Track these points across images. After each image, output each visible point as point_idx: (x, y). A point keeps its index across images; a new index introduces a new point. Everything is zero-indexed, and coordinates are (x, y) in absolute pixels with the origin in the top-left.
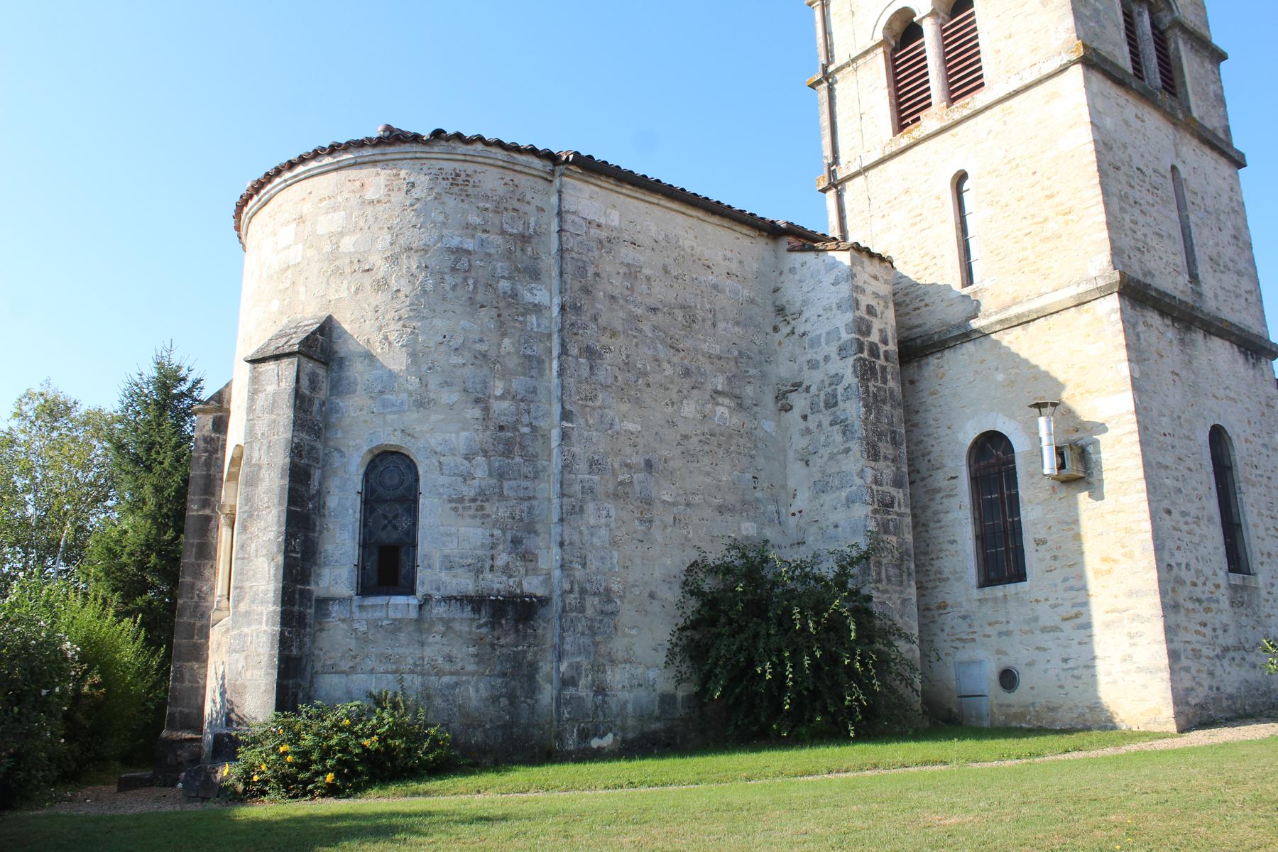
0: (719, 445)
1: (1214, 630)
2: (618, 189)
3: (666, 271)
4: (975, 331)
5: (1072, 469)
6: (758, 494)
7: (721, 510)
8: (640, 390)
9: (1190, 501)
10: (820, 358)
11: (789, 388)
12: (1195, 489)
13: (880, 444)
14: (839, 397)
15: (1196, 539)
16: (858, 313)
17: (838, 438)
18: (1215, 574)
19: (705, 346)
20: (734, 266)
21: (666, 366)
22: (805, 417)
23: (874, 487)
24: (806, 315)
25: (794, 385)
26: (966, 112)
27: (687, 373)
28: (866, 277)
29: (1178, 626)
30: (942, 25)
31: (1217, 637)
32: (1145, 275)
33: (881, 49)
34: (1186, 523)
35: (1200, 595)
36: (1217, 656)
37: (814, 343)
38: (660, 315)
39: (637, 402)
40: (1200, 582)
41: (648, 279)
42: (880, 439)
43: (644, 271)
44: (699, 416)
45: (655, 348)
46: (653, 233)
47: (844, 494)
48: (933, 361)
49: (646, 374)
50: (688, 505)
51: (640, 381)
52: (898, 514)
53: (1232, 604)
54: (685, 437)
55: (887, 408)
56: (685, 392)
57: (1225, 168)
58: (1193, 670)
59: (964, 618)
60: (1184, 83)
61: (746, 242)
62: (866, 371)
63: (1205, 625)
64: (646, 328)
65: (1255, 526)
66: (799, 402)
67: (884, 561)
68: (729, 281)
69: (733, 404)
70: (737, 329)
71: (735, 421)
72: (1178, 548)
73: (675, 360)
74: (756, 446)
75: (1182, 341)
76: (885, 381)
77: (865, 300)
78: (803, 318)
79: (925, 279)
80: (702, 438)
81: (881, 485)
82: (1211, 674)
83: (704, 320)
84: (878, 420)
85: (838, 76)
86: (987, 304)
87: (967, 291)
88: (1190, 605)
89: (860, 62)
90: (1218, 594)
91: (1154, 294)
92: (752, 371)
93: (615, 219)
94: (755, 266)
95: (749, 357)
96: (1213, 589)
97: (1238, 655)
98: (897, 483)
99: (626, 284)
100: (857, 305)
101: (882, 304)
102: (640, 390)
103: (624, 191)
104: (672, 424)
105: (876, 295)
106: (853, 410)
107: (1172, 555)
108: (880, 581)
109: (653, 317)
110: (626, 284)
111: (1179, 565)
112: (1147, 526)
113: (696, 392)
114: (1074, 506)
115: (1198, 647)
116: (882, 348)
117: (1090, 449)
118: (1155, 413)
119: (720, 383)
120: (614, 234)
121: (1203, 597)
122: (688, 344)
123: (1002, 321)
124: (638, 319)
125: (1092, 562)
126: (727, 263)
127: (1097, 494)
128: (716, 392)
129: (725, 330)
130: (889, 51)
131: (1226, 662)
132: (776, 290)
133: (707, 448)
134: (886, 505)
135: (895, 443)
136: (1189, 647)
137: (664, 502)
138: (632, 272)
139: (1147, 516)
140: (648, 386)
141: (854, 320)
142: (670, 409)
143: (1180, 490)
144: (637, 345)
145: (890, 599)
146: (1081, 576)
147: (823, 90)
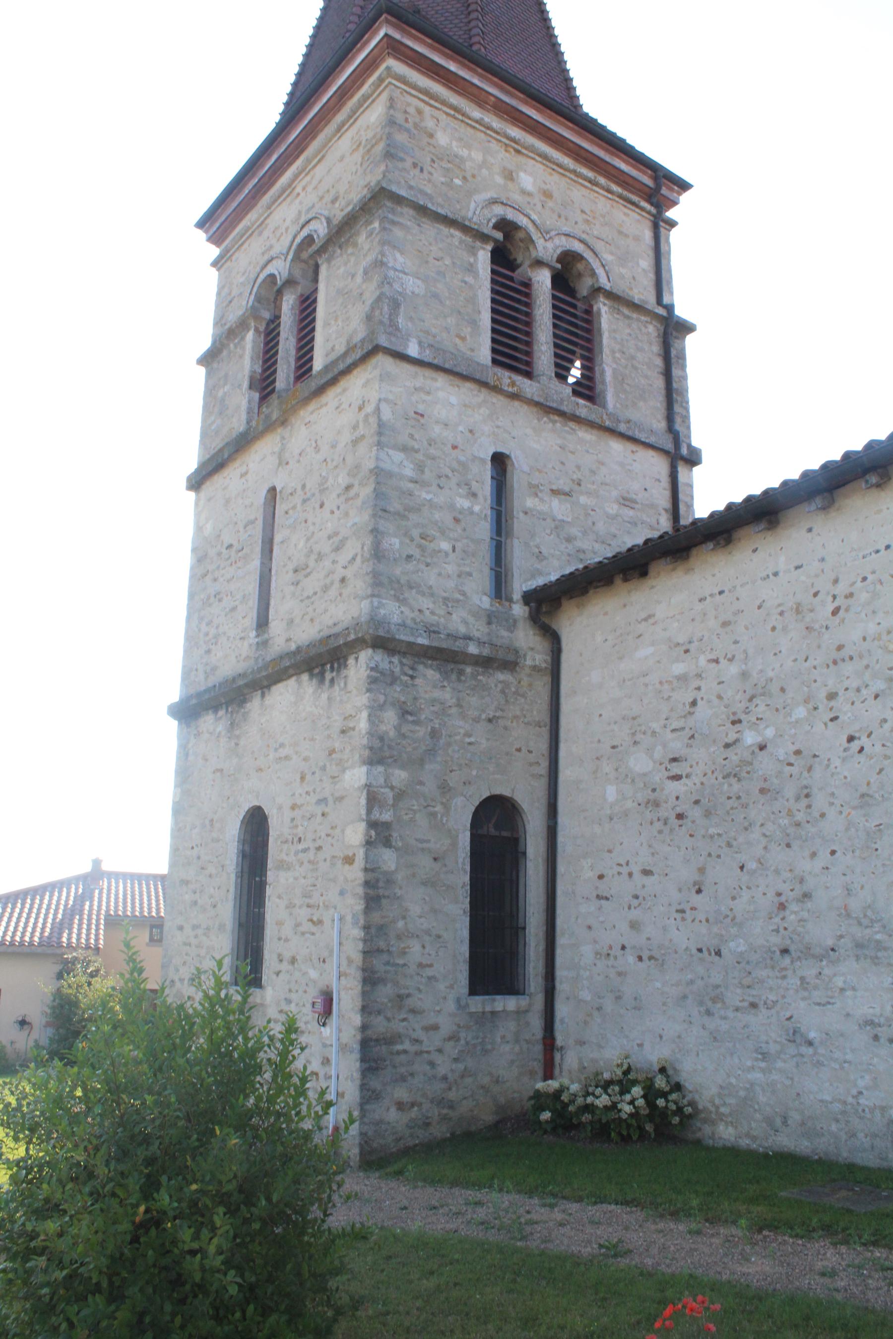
12: (211, 897)
65: (280, 923)
72: (184, 963)
75: (233, 725)
107: (177, 970)
111: (182, 980)
143: (196, 903)
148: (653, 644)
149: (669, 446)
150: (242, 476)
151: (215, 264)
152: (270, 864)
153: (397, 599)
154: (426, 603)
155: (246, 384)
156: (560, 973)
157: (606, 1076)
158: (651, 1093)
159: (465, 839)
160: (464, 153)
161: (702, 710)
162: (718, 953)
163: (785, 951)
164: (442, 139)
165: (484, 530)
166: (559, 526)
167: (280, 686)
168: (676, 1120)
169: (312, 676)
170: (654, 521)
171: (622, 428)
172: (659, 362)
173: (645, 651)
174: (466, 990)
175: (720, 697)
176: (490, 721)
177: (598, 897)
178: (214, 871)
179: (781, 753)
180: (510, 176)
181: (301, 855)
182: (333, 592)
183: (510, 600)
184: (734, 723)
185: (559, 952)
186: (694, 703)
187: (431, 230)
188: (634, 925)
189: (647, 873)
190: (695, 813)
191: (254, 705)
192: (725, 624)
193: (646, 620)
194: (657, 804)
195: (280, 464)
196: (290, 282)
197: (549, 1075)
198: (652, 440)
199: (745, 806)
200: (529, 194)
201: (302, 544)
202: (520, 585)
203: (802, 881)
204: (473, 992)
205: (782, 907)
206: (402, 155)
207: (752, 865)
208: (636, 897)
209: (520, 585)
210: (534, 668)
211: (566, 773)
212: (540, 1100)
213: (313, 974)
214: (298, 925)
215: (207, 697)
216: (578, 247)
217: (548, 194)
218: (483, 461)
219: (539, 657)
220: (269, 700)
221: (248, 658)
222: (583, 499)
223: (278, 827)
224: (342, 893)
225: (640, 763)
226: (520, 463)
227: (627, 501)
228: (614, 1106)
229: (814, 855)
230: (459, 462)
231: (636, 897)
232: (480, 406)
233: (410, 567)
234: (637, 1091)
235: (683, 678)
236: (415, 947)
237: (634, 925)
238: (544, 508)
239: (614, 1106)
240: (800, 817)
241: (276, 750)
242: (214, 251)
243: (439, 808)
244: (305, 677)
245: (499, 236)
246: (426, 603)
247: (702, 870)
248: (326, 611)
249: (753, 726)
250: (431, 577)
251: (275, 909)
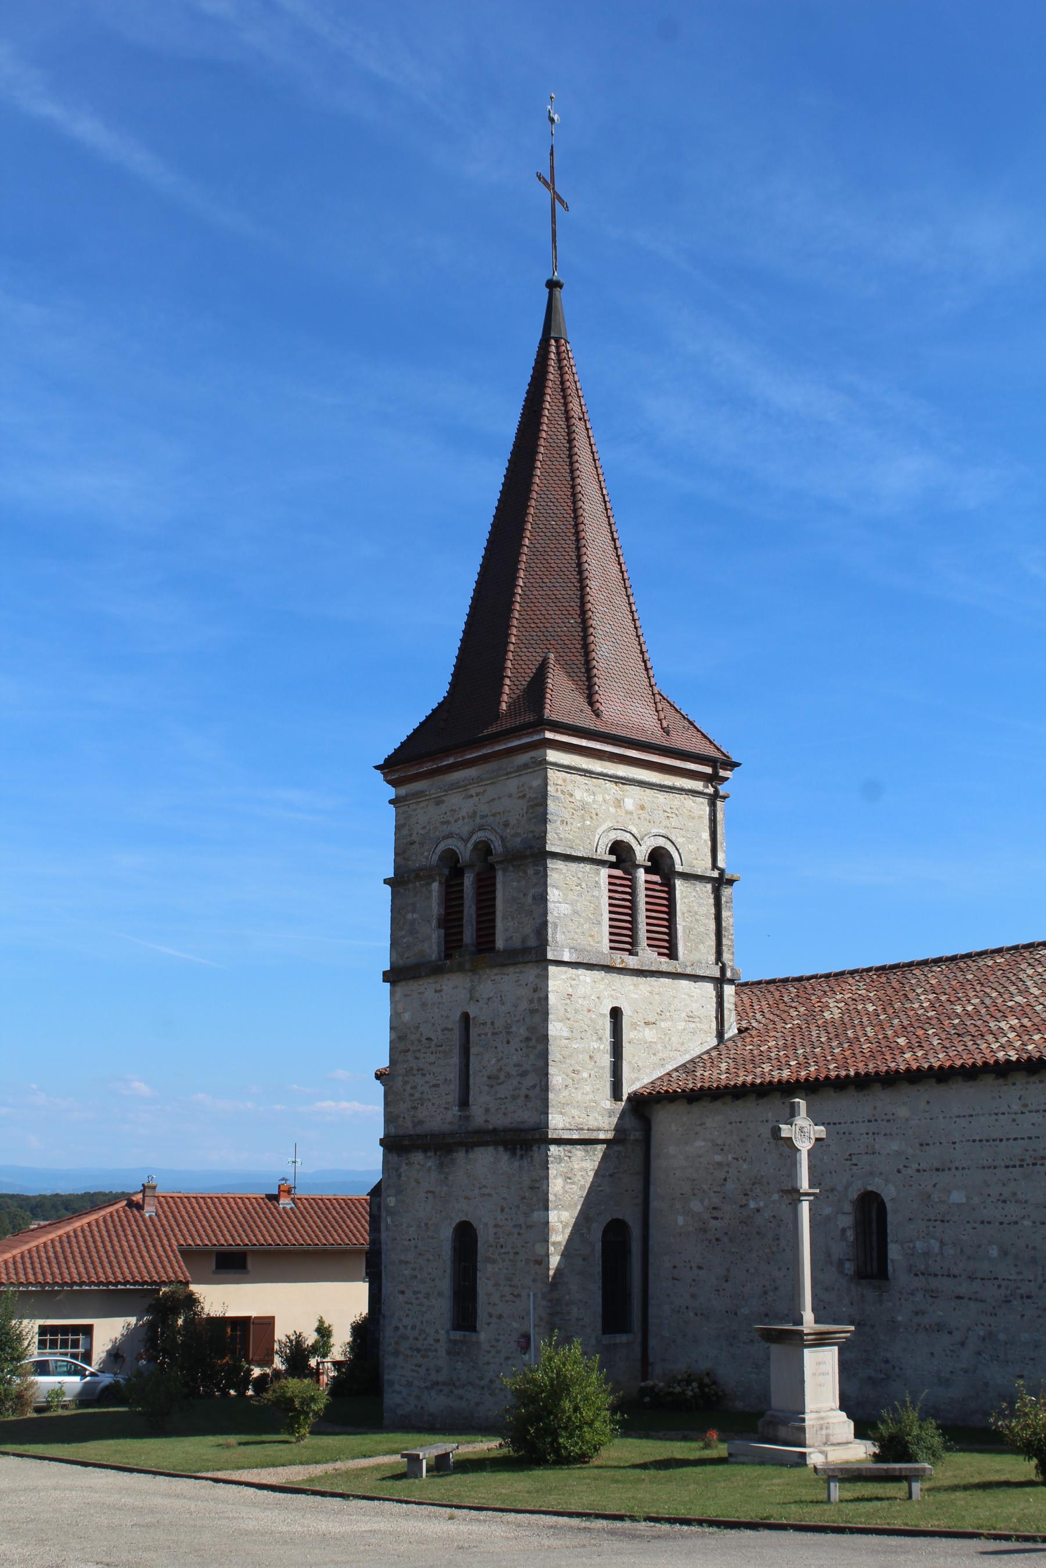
1: (428, 1370)
12: (429, 1274)
15: (424, 1309)
18: (437, 1332)
32: (414, 1126)
34: (417, 1299)
35: (420, 1346)
36: (426, 1387)
53: (448, 1353)
57: (530, 973)
63: (420, 1366)
75: (441, 1165)
82: (419, 1398)
88: (409, 1353)
91: (407, 1143)
107: (401, 1320)
111: (405, 1327)
115: (411, 1379)
143: (416, 1277)
148: (704, 1140)
149: (718, 975)
150: (436, 991)
151: (391, 802)
152: (479, 1258)
153: (561, 1113)
154: (575, 1112)
155: (434, 923)
156: (651, 1320)
157: (679, 1377)
158: (702, 1385)
159: (599, 1246)
160: (590, 799)
161: (730, 1186)
162: (736, 1314)
163: (766, 1315)
164: (578, 794)
165: (606, 1060)
166: (649, 1046)
167: (482, 1149)
168: (714, 1398)
169: (506, 1149)
170: (707, 1026)
171: (689, 971)
172: (713, 911)
173: (699, 1143)
174: (600, 1332)
175: (738, 1179)
176: (611, 1175)
177: (673, 1278)
178: (431, 1257)
179: (766, 1215)
180: (618, 803)
181: (503, 1256)
182: (520, 1101)
183: (621, 1100)
184: (746, 1195)
185: (650, 1308)
186: (725, 1179)
187: (573, 866)
188: (693, 1296)
189: (700, 1268)
190: (725, 1239)
191: (460, 1155)
192: (742, 1140)
193: (700, 1125)
194: (705, 1231)
195: (471, 998)
196: (471, 866)
197: (645, 1378)
198: (707, 973)
199: (749, 1240)
200: (631, 813)
201: (493, 1061)
202: (627, 1090)
203: (774, 1281)
204: (604, 1333)
205: (765, 1293)
206: (555, 818)
207: (752, 1270)
208: (694, 1280)
209: (627, 1090)
210: (636, 1140)
211: (655, 1204)
212: (643, 1392)
213: (515, 1325)
214: (503, 1296)
216: (661, 842)
217: (642, 808)
218: (604, 1015)
219: (637, 1133)
220: (471, 1156)
221: (450, 1123)
222: (663, 1025)
223: (485, 1236)
224: (534, 1280)
225: (696, 1206)
226: (627, 1012)
227: (690, 1018)
228: (683, 1392)
229: (780, 1269)
230: (591, 1019)
231: (694, 1280)
232: (603, 979)
233: (565, 1093)
234: (695, 1384)
235: (720, 1164)
236: (575, 1310)
237: (693, 1296)
238: (641, 1035)
239: (683, 1392)
240: (774, 1249)
241: (480, 1188)
242: (391, 792)
243: (585, 1231)
244: (501, 1149)
245: (613, 858)
246: (575, 1112)
247: (728, 1270)
248: (515, 1112)
249: (754, 1199)
250: (579, 1096)
251: (484, 1286)
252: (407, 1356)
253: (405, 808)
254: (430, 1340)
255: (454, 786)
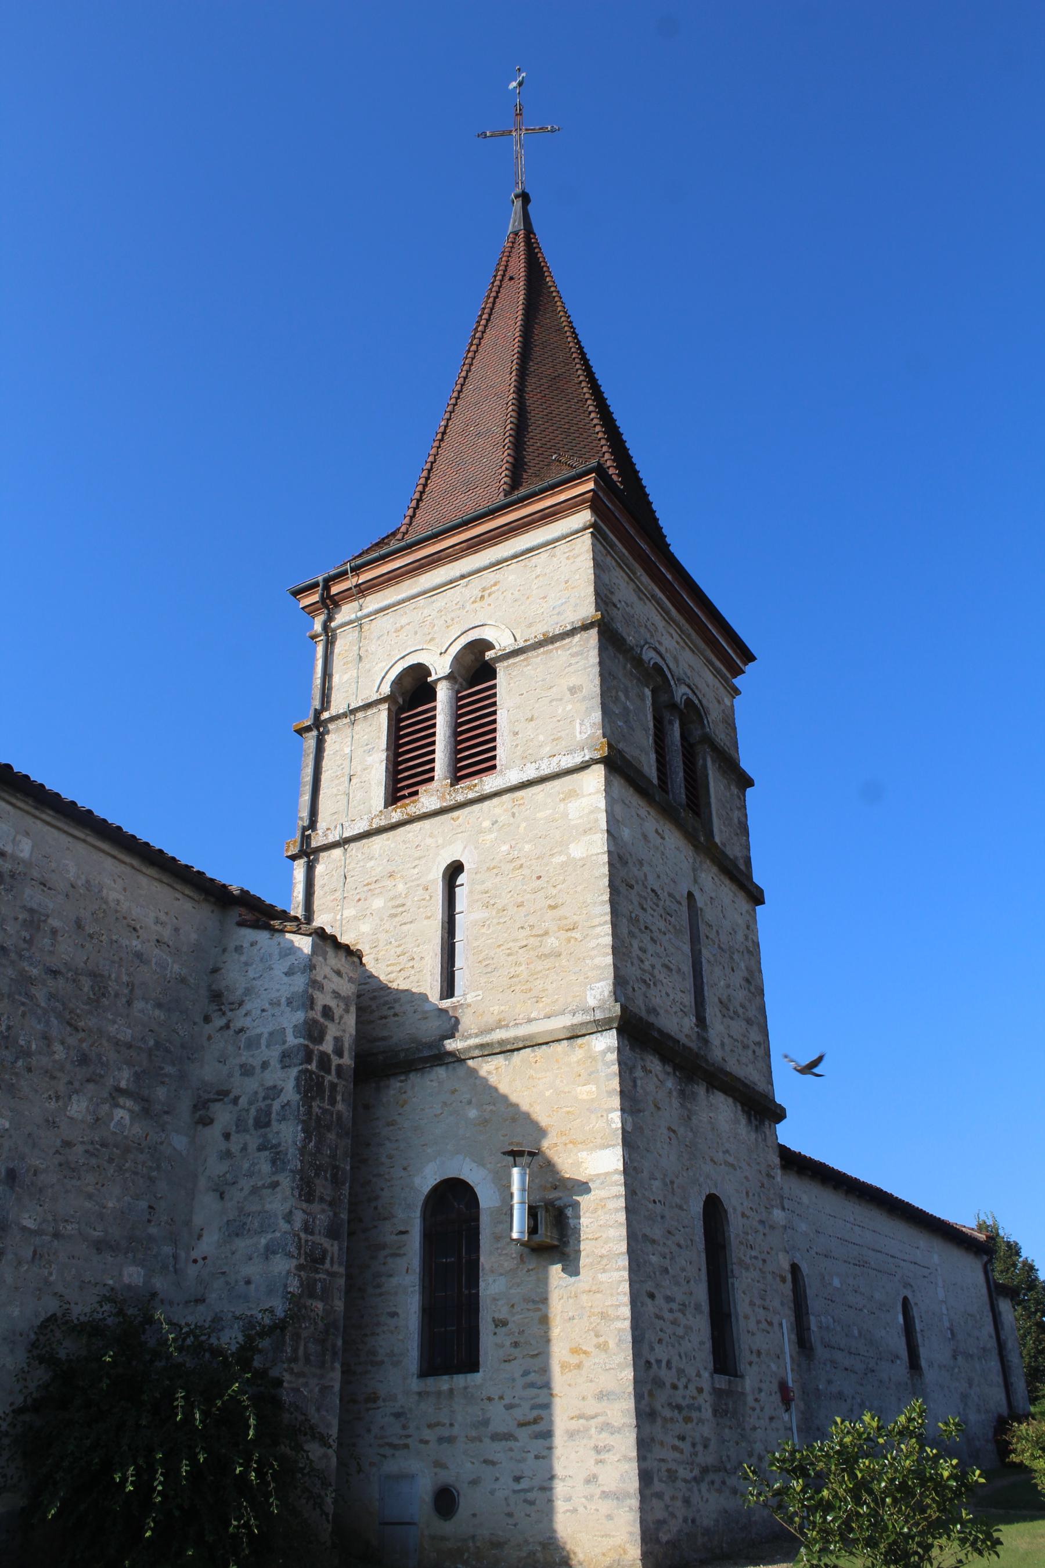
0: (111, 1160)
1: (694, 1445)
2: (37, 813)
3: (79, 925)
4: (451, 1054)
5: (546, 1234)
6: (153, 1230)
7: (100, 1246)
8: (16, 1074)
9: (678, 1284)
10: (257, 1062)
11: (212, 1096)
12: (683, 1270)
13: (317, 1181)
14: (274, 1116)
15: (680, 1331)
16: (312, 1014)
17: (266, 1167)
18: (699, 1375)
19: (112, 1029)
20: (166, 933)
21: (57, 1047)
22: (227, 1136)
23: (303, 1235)
24: (248, 1006)
25: (219, 1093)
26: (471, 795)
27: (84, 1060)
28: (327, 970)
29: (653, 1440)
30: (458, 692)
31: (696, 1454)
33: (386, 706)
34: (671, 1311)
35: (680, 1401)
36: (695, 1479)
37: (253, 1043)
38: (61, 981)
39: (12, 1090)
40: (681, 1386)
41: (54, 932)
42: (317, 1175)
43: (50, 921)
44: (90, 1119)
45: (48, 1023)
46: (71, 876)
47: (263, 1241)
48: (395, 1084)
49: (27, 1053)
50: (56, 1235)
51: (20, 1063)
52: (329, 1273)
53: (715, 1412)
54: (67, 1144)
55: (331, 1136)
56: (77, 1085)
58: (667, 1498)
59: (397, 1415)
60: (709, 804)
61: (188, 905)
62: (311, 1087)
64: (40, 994)
65: (746, 1317)
66: (223, 1116)
67: (304, 1334)
68: (156, 951)
69: (137, 1108)
70: (157, 1012)
71: (137, 1130)
72: (660, 1341)
73: (71, 1041)
74: (158, 1168)
75: (682, 1093)
76: (333, 1102)
77: (323, 999)
78: (242, 1011)
79: (399, 983)
80: (90, 1148)
81: (312, 1233)
82: (687, 1501)
83: (117, 995)
84: (318, 1149)
85: (331, 726)
86: (468, 1022)
87: (446, 1004)
88: (667, 1413)
89: (360, 715)
90: (700, 1400)
91: (656, 1034)
92: (169, 1069)
93: (25, 849)
94: (194, 936)
95: (167, 1051)
96: (695, 1393)
97: (717, 1477)
98: (333, 1233)
99: (24, 934)
100: (311, 1003)
101: (342, 1006)
102: (16, 1074)
103: (44, 816)
104: (52, 1124)
105: (336, 995)
106: (289, 1134)
107: (652, 1349)
108: (294, 1359)
109: (51, 982)
110: (24, 934)
111: (659, 1362)
112: (626, 1311)
113: (91, 1086)
114: (544, 1281)
115: (673, 1466)
116: (335, 1061)
117: (569, 1212)
118: (645, 1174)
119: (124, 1078)
120: (21, 868)
121: (684, 1404)
122: (92, 1022)
123: (482, 1046)
124: (31, 981)
125: (559, 1352)
126: (159, 928)
127: (572, 1268)
128: (119, 1090)
129: (142, 1011)
130: (394, 709)
131: (704, 1487)
132: (215, 970)
133: (93, 1161)
134: (314, 1260)
135: (336, 1182)
136: (664, 1467)
137: (24, 1229)
138: (34, 921)
139: (626, 1299)
140: (30, 1070)
141: (306, 1022)
142: (53, 1105)
143: (666, 1271)
144: (24, 1015)
145: (306, 1385)
146: (545, 1370)
147: (310, 741)
215: (671, 1044)
252: (665, 1419)
253: (604, 552)
254: (692, 1388)
255: (659, 602)
